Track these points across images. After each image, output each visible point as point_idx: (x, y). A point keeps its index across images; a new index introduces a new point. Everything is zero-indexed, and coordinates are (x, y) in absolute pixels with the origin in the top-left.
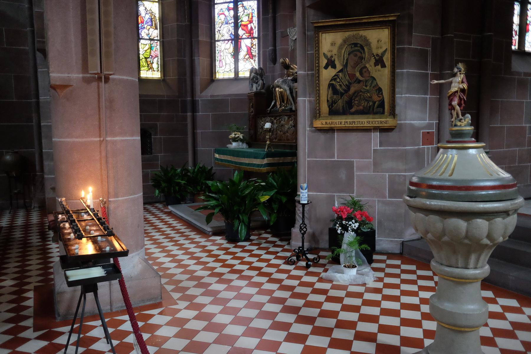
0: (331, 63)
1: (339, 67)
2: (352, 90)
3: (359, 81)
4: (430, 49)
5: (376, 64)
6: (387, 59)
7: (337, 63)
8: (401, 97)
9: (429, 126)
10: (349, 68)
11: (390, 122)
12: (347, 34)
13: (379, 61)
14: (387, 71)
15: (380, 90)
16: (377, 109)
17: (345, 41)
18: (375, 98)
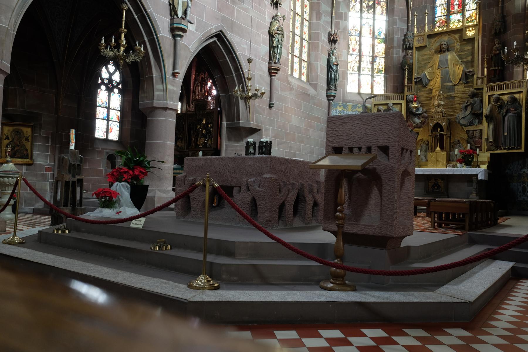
0: (7, 138)
1: (11, 140)
2: (16, 149)
3: (19, 146)
4: (50, 136)
5: (26, 140)
6: (30, 138)
7: (10, 138)
8: (35, 153)
9: (50, 165)
10: (15, 141)
11: (30, 162)
12: (14, 128)
13: (27, 139)
14: (30, 143)
15: (27, 150)
16: (26, 157)
17: (14, 130)
18: (25, 152)
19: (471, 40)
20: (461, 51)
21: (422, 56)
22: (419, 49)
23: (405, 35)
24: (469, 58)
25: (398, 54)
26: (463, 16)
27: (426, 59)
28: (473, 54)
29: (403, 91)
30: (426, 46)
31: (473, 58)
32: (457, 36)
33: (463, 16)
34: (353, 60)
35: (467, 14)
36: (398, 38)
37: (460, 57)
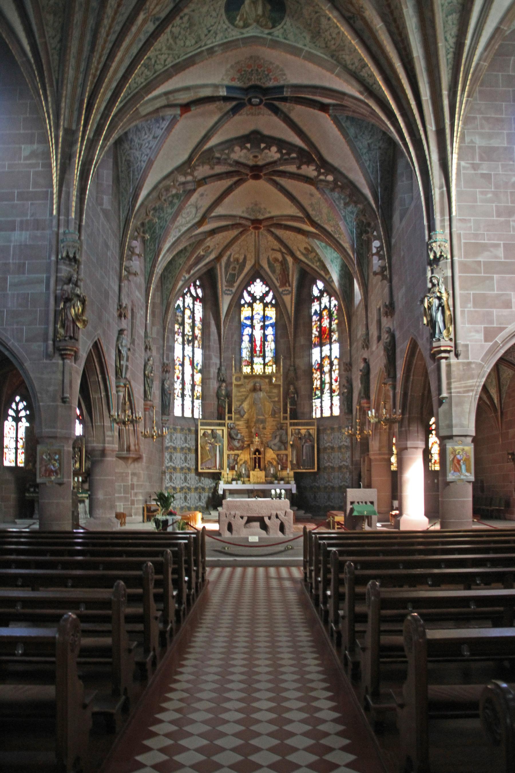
19: (277, 386)
20: (270, 392)
21: (239, 392)
22: (237, 386)
23: (219, 369)
24: (276, 399)
25: (214, 385)
26: (264, 359)
27: (243, 395)
28: (279, 396)
29: (224, 419)
30: (242, 385)
31: (280, 399)
32: (267, 380)
33: (264, 359)
34: (178, 386)
35: (267, 360)
36: (214, 371)
37: (270, 397)
